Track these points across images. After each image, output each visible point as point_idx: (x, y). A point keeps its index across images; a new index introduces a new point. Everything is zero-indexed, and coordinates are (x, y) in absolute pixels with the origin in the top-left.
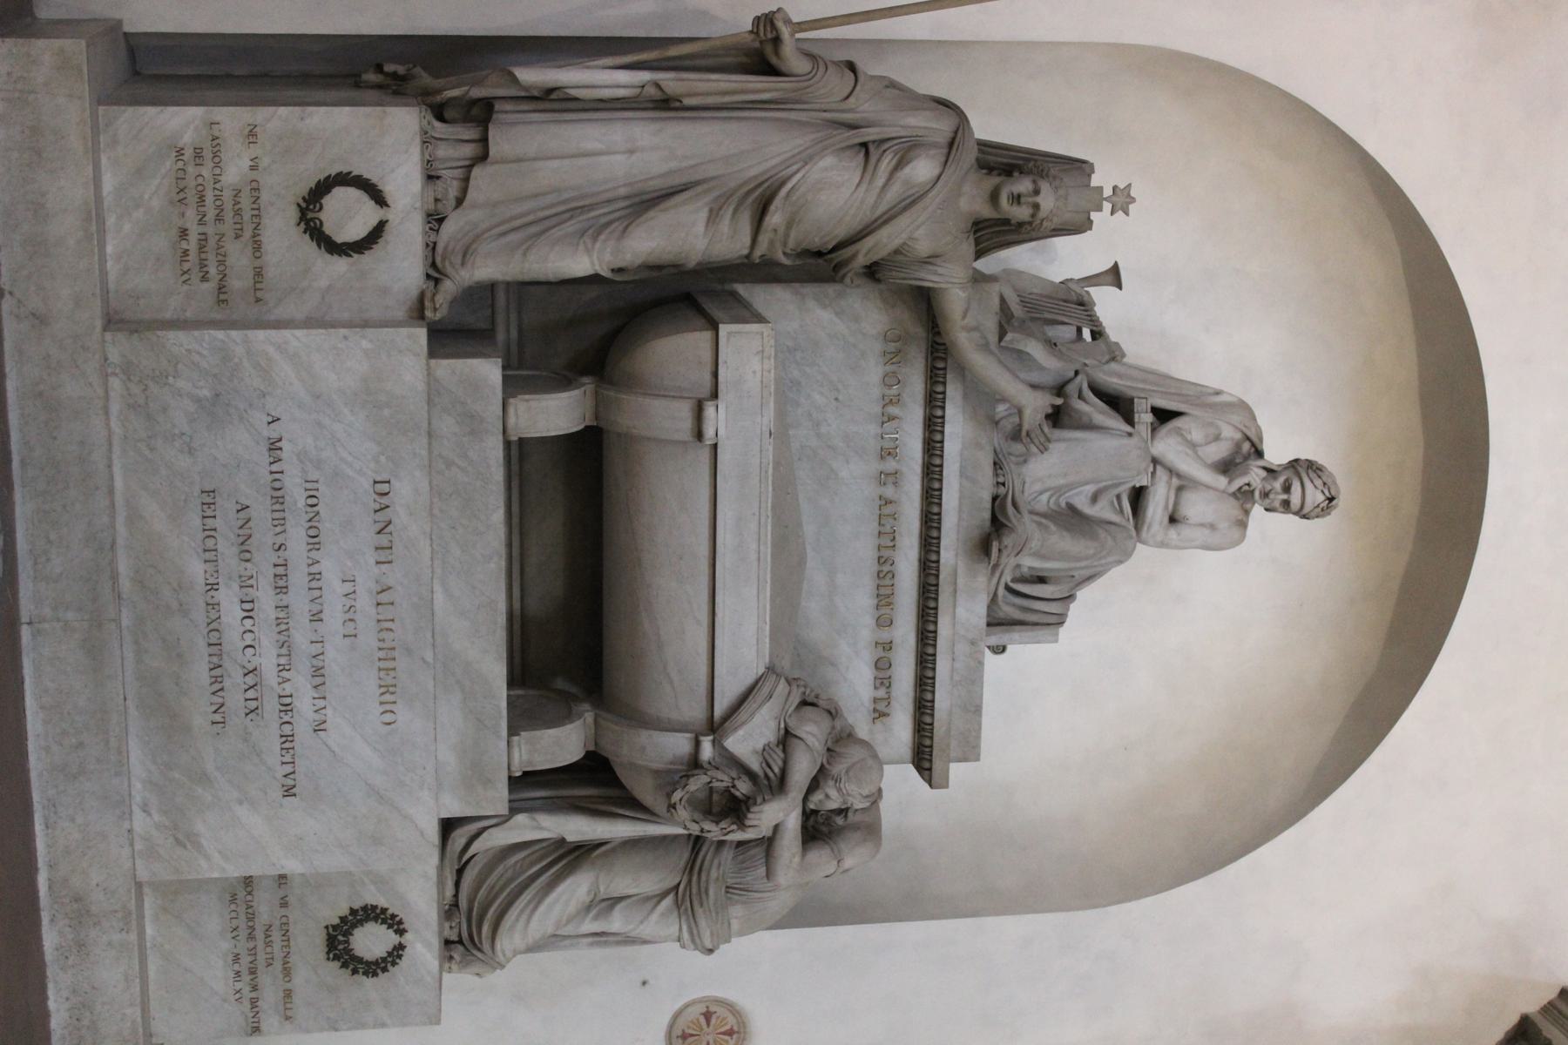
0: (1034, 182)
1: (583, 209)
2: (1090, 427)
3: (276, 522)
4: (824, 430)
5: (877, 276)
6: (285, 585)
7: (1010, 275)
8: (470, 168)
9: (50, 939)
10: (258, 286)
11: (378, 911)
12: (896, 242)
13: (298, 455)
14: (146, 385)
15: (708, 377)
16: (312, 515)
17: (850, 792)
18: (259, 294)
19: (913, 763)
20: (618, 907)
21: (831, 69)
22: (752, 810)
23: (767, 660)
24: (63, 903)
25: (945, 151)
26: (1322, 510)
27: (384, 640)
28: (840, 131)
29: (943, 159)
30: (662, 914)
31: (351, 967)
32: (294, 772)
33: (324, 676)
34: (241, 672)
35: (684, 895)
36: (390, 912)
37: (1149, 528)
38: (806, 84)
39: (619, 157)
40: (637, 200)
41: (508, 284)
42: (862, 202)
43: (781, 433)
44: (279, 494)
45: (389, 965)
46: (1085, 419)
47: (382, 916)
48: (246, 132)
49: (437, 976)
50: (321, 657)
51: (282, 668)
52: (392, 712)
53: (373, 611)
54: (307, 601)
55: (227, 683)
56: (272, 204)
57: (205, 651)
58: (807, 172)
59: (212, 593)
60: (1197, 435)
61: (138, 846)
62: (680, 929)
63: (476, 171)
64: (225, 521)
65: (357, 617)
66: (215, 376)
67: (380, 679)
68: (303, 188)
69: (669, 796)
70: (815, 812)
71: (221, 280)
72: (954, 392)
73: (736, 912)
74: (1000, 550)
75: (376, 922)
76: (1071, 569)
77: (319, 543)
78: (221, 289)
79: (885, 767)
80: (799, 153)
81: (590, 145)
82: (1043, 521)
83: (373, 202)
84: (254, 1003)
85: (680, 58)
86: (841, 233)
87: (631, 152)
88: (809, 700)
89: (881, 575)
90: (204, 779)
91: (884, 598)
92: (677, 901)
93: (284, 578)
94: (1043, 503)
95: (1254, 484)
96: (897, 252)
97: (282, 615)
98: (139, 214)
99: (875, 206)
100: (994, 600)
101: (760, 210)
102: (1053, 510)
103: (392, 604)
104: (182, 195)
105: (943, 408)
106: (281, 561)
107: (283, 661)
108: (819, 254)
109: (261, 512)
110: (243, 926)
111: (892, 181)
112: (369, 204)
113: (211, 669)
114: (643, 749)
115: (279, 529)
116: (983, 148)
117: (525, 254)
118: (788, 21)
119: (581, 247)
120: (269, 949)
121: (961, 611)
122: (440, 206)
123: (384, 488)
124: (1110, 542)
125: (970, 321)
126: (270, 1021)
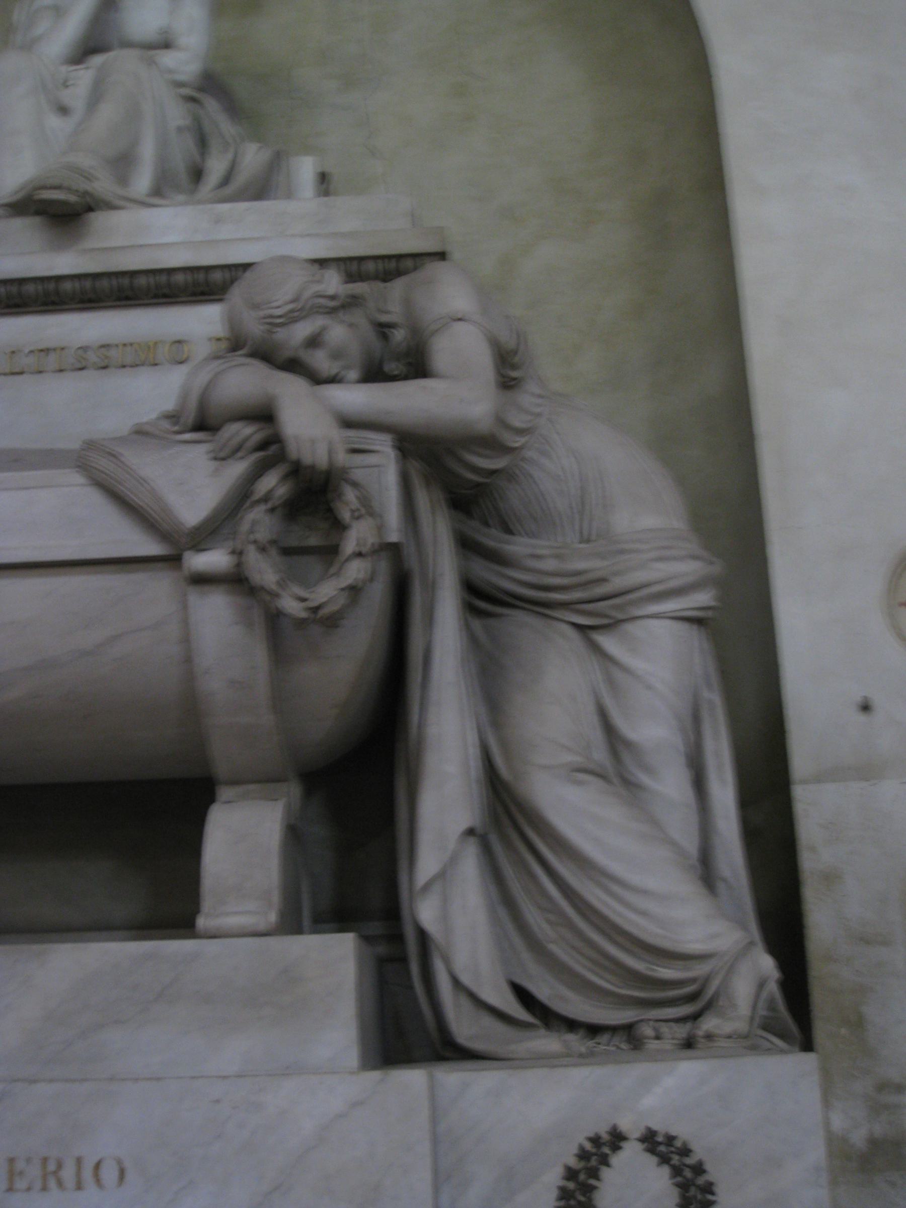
11: (571, 1185)
17: (289, 297)
36: (573, 1162)
45: (689, 1161)
47: (582, 1177)
52: (97, 1166)
67: (29, 1189)
69: (301, 623)
75: (593, 1188)
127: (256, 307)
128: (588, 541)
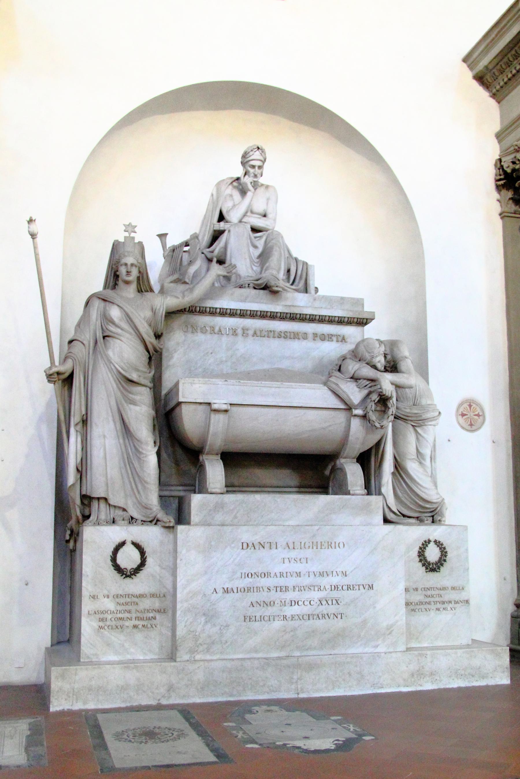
0: (121, 265)
1: (129, 458)
2: (225, 248)
3: (258, 591)
4: (224, 359)
5: (160, 334)
6: (285, 588)
7: (161, 280)
8: (109, 504)
9: (428, 686)
10: (158, 596)
11: (420, 551)
12: (146, 325)
13: (230, 581)
14: (199, 644)
15: (201, 407)
16: (256, 576)
18: (162, 595)
19: (363, 326)
20: (420, 450)
21: (72, 350)
22: (385, 394)
23: (322, 385)
24: (414, 681)
25: (107, 303)
26: (263, 152)
27: (309, 546)
28: (98, 349)
29: (111, 304)
30: (424, 433)
31: (443, 562)
32: (363, 585)
33: (323, 572)
34: (321, 606)
35: (417, 423)
36: (421, 546)
37: (267, 226)
38: (77, 361)
39: (107, 442)
40: (125, 436)
41: (160, 490)
42: (128, 338)
43: (226, 377)
44: (246, 589)
45: (442, 546)
46: (222, 250)
47: (423, 549)
48: (92, 599)
49: (448, 527)
50: (315, 573)
51: (320, 589)
53: (297, 550)
54: (292, 578)
55: (325, 612)
56: (124, 590)
57: (311, 621)
58: (115, 362)
59: (287, 618)
60: (230, 204)
61: (392, 650)
62: (430, 425)
63: (111, 503)
64: (258, 611)
65: (299, 558)
66: (196, 615)
68: (117, 575)
69: (377, 428)
70: (385, 367)
71: (155, 612)
72: (210, 304)
73: (424, 402)
74: (277, 287)
75: (425, 551)
76: (285, 258)
77: (268, 573)
78: (159, 611)
79: (365, 337)
80: (107, 365)
81: (102, 454)
82: (264, 268)
83: (124, 547)
84: (456, 602)
85: (65, 416)
86: (141, 348)
87: (104, 437)
88: (338, 368)
89: (285, 337)
90: (365, 622)
91: (296, 336)
92: (419, 426)
93: (282, 588)
94: (256, 268)
95: (251, 181)
96: (150, 325)
97: (297, 589)
98: (127, 645)
99: (130, 334)
100: (297, 290)
101: (131, 383)
102: (260, 265)
103: (294, 543)
104: (119, 627)
105: (216, 308)
106: (275, 589)
107: (316, 589)
108: (150, 358)
109: (253, 597)
110: (425, 606)
111: (119, 326)
112: (124, 547)
113: (319, 619)
114: (357, 439)
115: (261, 589)
116: (107, 287)
117: (147, 483)
118: (50, 368)
119: (145, 459)
120: (435, 596)
121: (302, 304)
122: (126, 518)
123: (245, 545)
124: (273, 241)
125: (180, 296)
126: (463, 596)
127: (369, 353)
128: (416, 405)
